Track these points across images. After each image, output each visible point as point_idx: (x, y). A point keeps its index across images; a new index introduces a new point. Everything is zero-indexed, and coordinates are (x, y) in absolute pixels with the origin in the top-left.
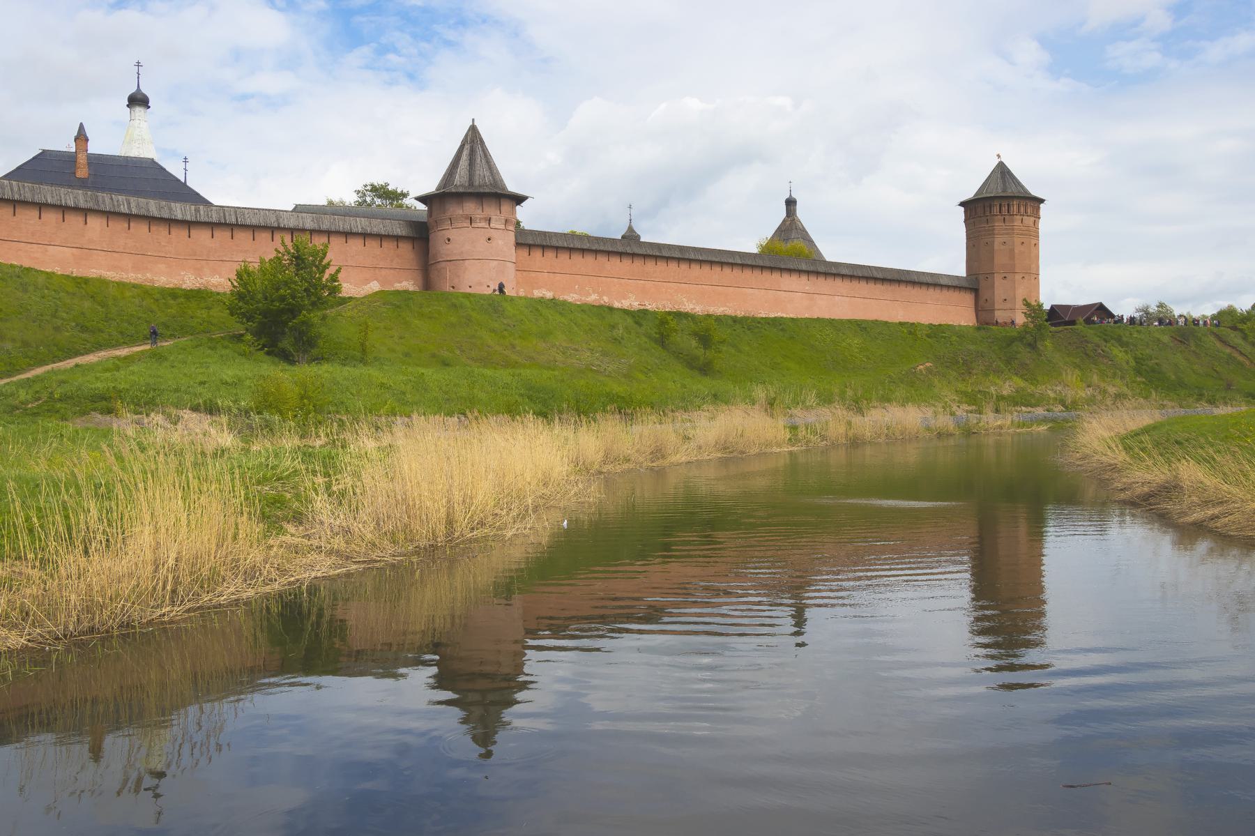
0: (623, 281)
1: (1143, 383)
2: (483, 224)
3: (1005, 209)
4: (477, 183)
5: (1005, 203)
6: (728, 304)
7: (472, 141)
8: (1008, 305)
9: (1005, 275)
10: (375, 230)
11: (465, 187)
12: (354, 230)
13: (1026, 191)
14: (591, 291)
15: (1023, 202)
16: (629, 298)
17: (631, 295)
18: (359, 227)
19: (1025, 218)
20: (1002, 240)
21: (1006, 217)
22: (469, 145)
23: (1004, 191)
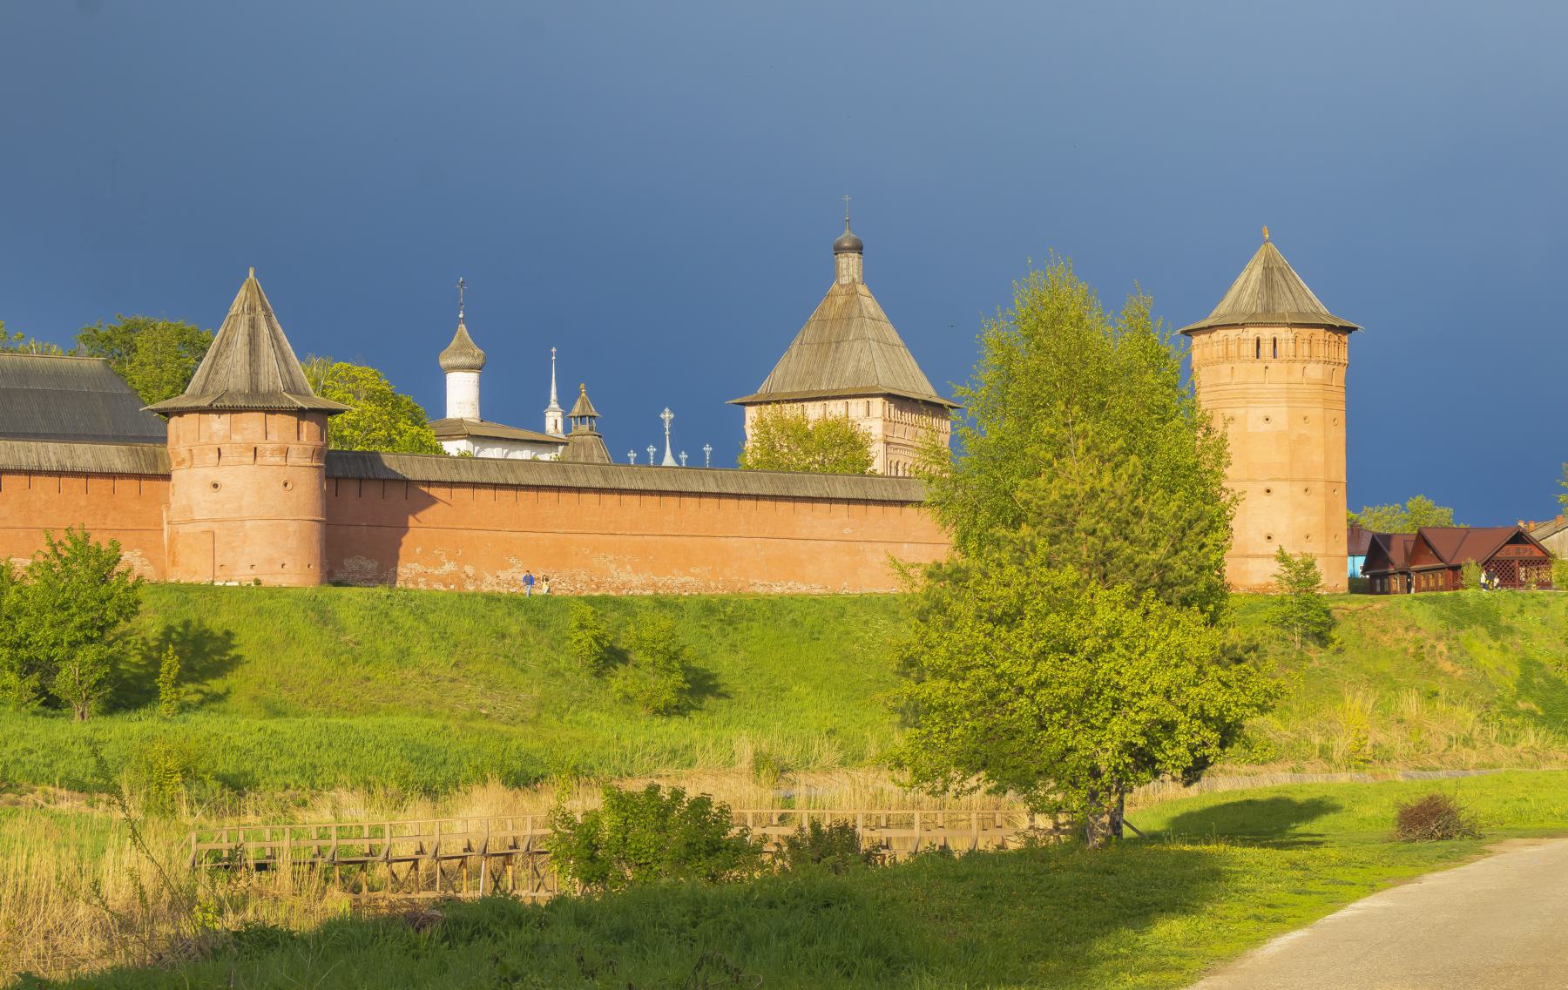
0: (500, 534)
1: (1532, 714)
2: (278, 459)
3: (1266, 348)
4: (263, 388)
5: (1266, 334)
6: (692, 570)
7: (252, 309)
9: (1269, 485)
10: (81, 465)
11: (246, 396)
12: (45, 467)
14: (443, 558)
15: (1306, 332)
16: (512, 566)
17: (513, 560)
18: (53, 459)
19: (1310, 366)
20: (1262, 412)
21: (1271, 366)
22: (247, 317)
23: (1267, 311)
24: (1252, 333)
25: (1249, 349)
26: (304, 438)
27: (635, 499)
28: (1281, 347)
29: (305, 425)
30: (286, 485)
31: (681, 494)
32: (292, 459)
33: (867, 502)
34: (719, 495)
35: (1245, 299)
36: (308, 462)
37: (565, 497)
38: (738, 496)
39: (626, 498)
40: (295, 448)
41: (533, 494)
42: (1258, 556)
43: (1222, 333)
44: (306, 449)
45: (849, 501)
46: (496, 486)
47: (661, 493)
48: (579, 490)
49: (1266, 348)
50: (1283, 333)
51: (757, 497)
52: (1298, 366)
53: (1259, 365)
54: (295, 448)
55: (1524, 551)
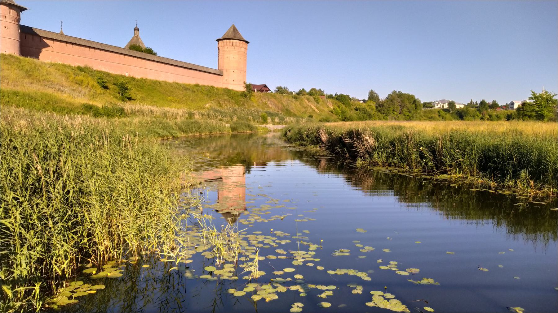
3: (234, 44)
5: (235, 41)
8: (235, 83)
13: (243, 38)
24: (232, 41)
25: (231, 44)
26: (11, 14)
27: (109, 53)
28: (237, 44)
29: (12, 11)
30: (5, 27)
31: (120, 54)
32: (7, 20)
33: (161, 63)
34: (129, 56)
35: (230, 34)
36: (13, 22)
37: (91, 50)
38: (133, 57)
39: (107, 53)
40: (8, 16)
41: (82, 48)
42: (231, 84)
43: (225, 40)
44: (12, 18)
45: (157, 62)
46: (73, 44)
47: (115, 53)
48: (95, 48)
49: (234, 44)
50: (237, 41)
51: (138, 57)
52: (240, 48)
53: (233, 47)
54: (8, 16)
55: (266, 89)
